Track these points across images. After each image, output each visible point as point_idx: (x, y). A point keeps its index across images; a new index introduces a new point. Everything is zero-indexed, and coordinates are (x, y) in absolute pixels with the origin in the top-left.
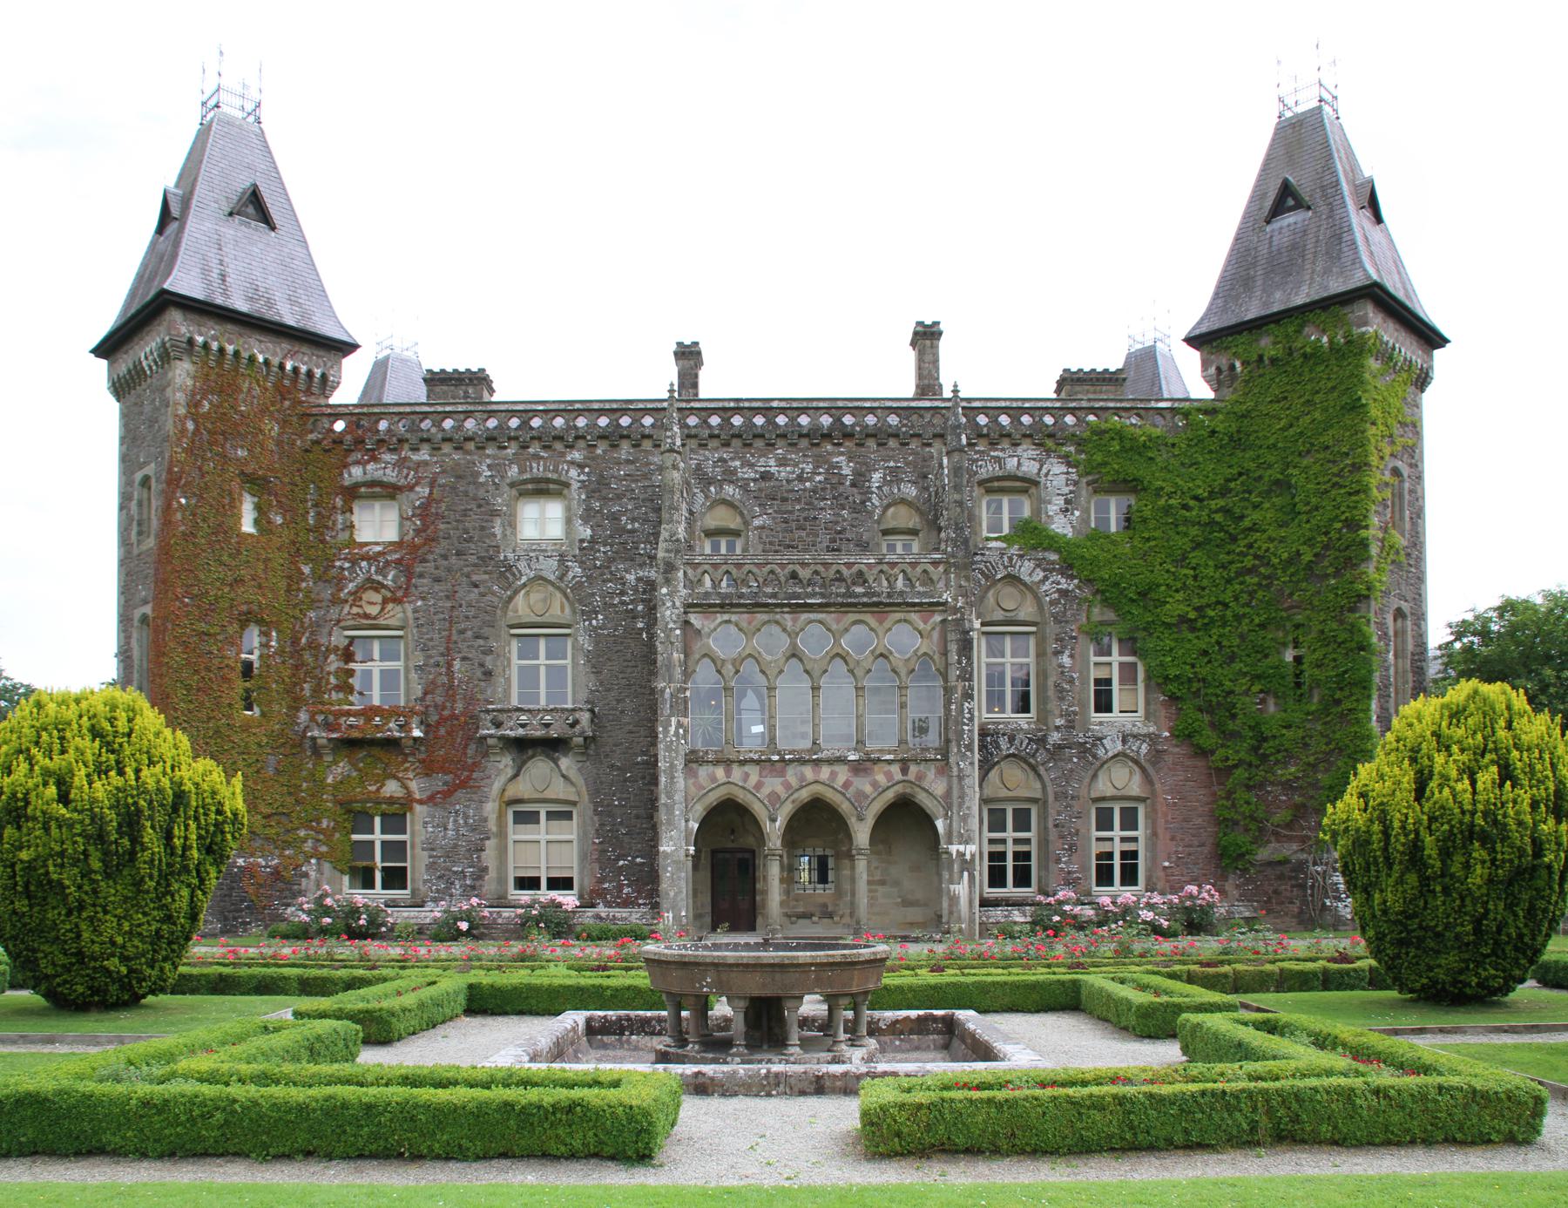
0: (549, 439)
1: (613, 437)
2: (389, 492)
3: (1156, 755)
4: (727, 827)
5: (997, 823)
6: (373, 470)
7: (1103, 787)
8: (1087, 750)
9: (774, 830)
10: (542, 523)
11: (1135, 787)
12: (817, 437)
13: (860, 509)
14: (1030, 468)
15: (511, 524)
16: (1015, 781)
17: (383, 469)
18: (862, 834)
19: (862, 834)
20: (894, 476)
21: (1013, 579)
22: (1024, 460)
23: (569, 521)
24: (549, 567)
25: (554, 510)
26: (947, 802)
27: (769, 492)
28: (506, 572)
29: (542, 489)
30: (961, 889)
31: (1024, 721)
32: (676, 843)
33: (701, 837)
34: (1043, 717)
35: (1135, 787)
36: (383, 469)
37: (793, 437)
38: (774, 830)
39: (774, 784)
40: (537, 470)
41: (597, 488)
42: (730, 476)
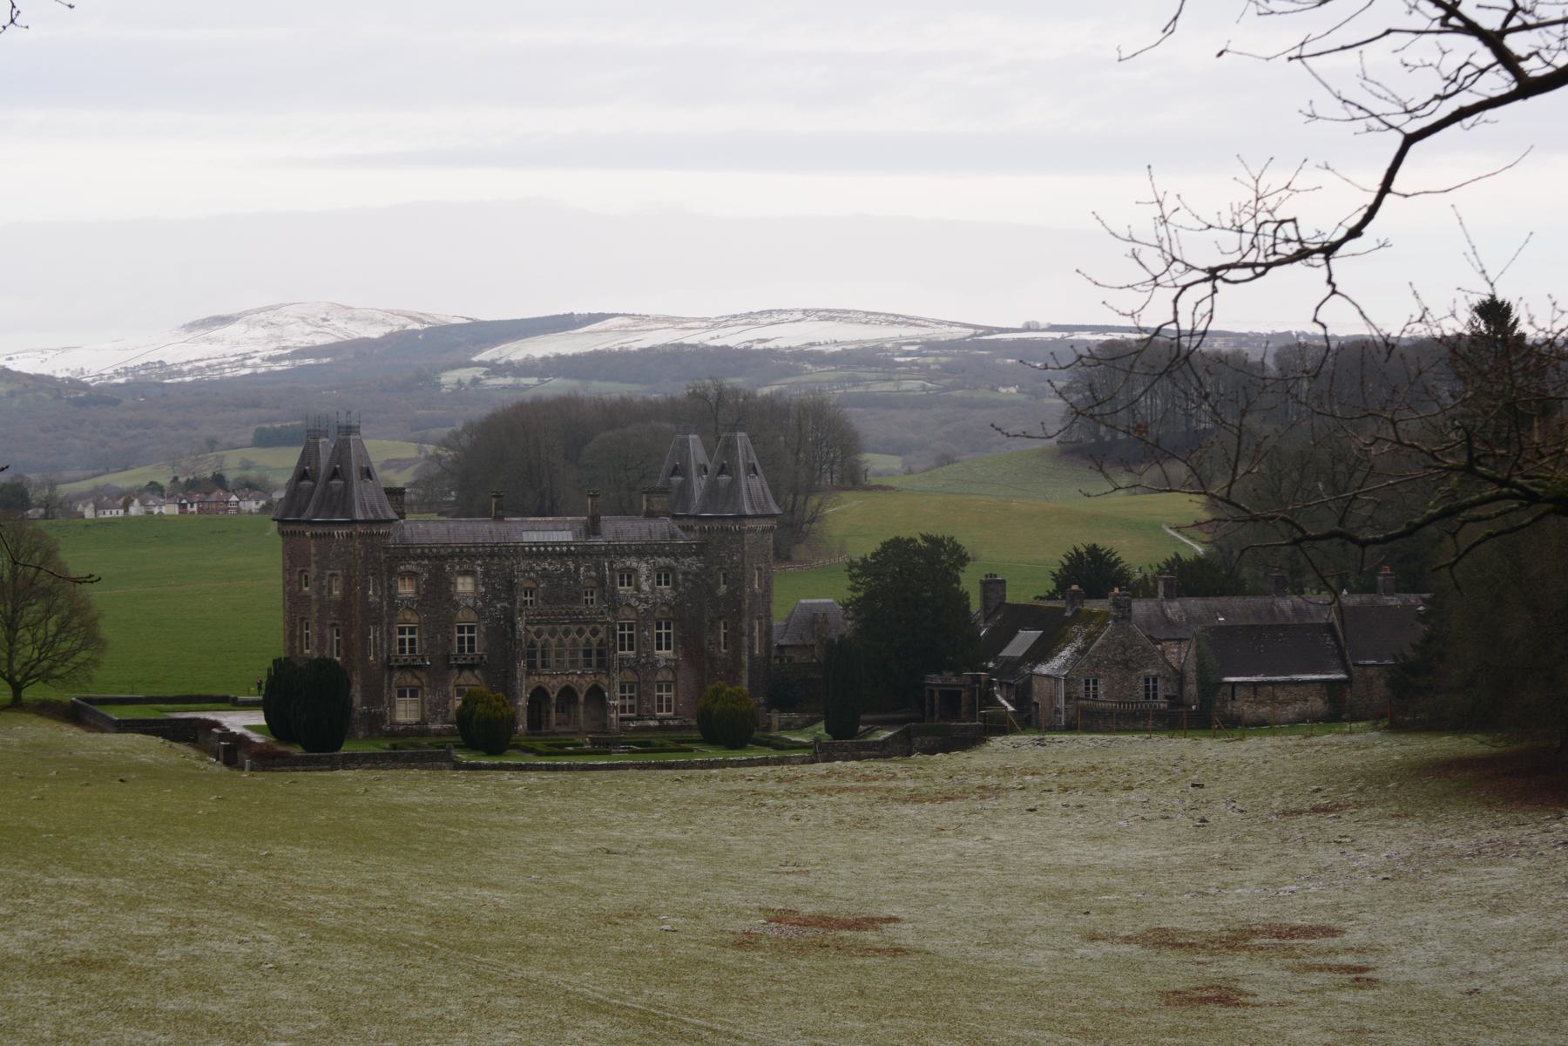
0: (470, 556)
1: (492, 555)
2: (412, 575)
3: (677, 667)
4: (539, 696)
5: (623, 690)
6: (409, 567)
7: (659, 678)
8: (654, 664)
9: (554, 696)
10: (465, 585)
11: (670, 678)
12: (561, 554)
13: (576, 580)
14: (635, 565)
15: (455, 585)
16: (630, 676)
17: (412, 567)
18: (582, 698)
19: (582, 698)
20: (588, 569)
21: (629, 605)
22: (632, 562)
23: (476, 585)
24: (470, 602)
25: (469, 580)
26: (609, 687)
27: (546, 575)
28: (456, 606)
29: (466, 573)
30: (613, 716)
31: (632, 654)
32: (522, 702)
33: (530, 701)
34: (638, 653)
35: (670, 678)
36: (412, 567)
37: (554, 555)
38: (554, 696)
39: (554, 682)
40: (466, 567)
41: (486, 574)
42: (532, 569)
